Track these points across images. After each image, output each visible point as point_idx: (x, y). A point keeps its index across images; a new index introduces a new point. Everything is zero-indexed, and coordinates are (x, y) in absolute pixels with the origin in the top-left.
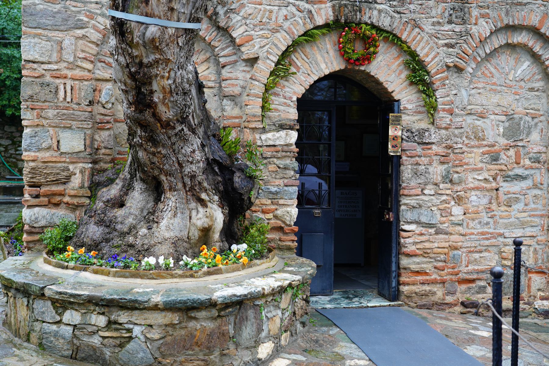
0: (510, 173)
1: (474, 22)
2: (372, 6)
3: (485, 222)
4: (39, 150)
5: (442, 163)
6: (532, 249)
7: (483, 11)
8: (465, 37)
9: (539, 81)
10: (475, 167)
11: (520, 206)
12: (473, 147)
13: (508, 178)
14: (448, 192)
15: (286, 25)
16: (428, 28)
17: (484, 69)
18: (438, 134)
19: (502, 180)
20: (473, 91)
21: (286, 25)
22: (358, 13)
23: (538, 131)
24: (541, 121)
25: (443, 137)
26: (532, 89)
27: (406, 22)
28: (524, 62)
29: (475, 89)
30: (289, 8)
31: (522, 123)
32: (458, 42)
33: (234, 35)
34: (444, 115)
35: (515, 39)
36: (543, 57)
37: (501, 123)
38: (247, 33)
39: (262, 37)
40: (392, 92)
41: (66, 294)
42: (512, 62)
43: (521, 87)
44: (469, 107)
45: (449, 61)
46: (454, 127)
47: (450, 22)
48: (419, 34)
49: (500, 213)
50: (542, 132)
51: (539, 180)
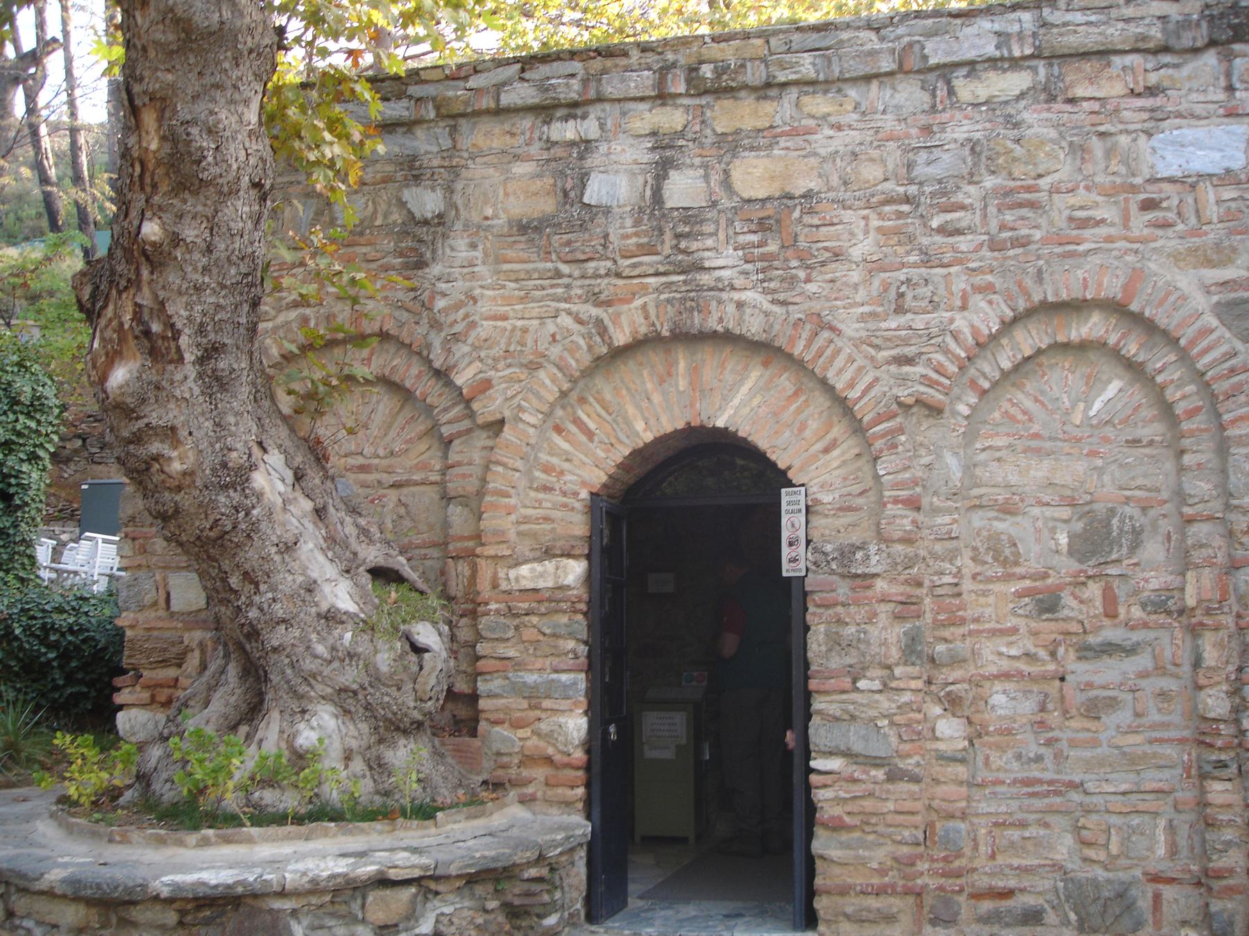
0: (1091, 639)
2: (724, 295)
3: (1032, 755)
4: (142, 609)
5: (898, 617)
6: (1162, 823)
7: (979, 280)
8: (940, 339)
9: (1151, 421)
10: (999, 626)
11: (1124, 717)
12: (989, 580)
13: (1087, 652)
14: (914, 684)
15: (555, 351)
16: (851, 328)
17: (1006, 405)
18: (884, 555)
19: (1072, 655)
20: (983, 457)
21: (555, 351)
22: (696, 313)
23: (1160, 538)
24: (1164, 516)
25: (898, 560)
26: (1135, 442)
27: (800, 319)
28: (1109, 382)
29: (987, 452)
30: (559, 320)
31: (1115, 522)
32: (924, 350)
33: (460, 380)
34: (899, 512)
36: (1150, 368)
37: (1059, 524)
38: (481, 375)
39: (510, 380)
40: (789, 468)
42: (1075, 381)
43: (1106, 440)
44: (976, 492)
45: (903, 393)
46: (932, 537)
47: (900, 310)
48: (831, 341)
49: (1069, 734)
51: (1168, 654)
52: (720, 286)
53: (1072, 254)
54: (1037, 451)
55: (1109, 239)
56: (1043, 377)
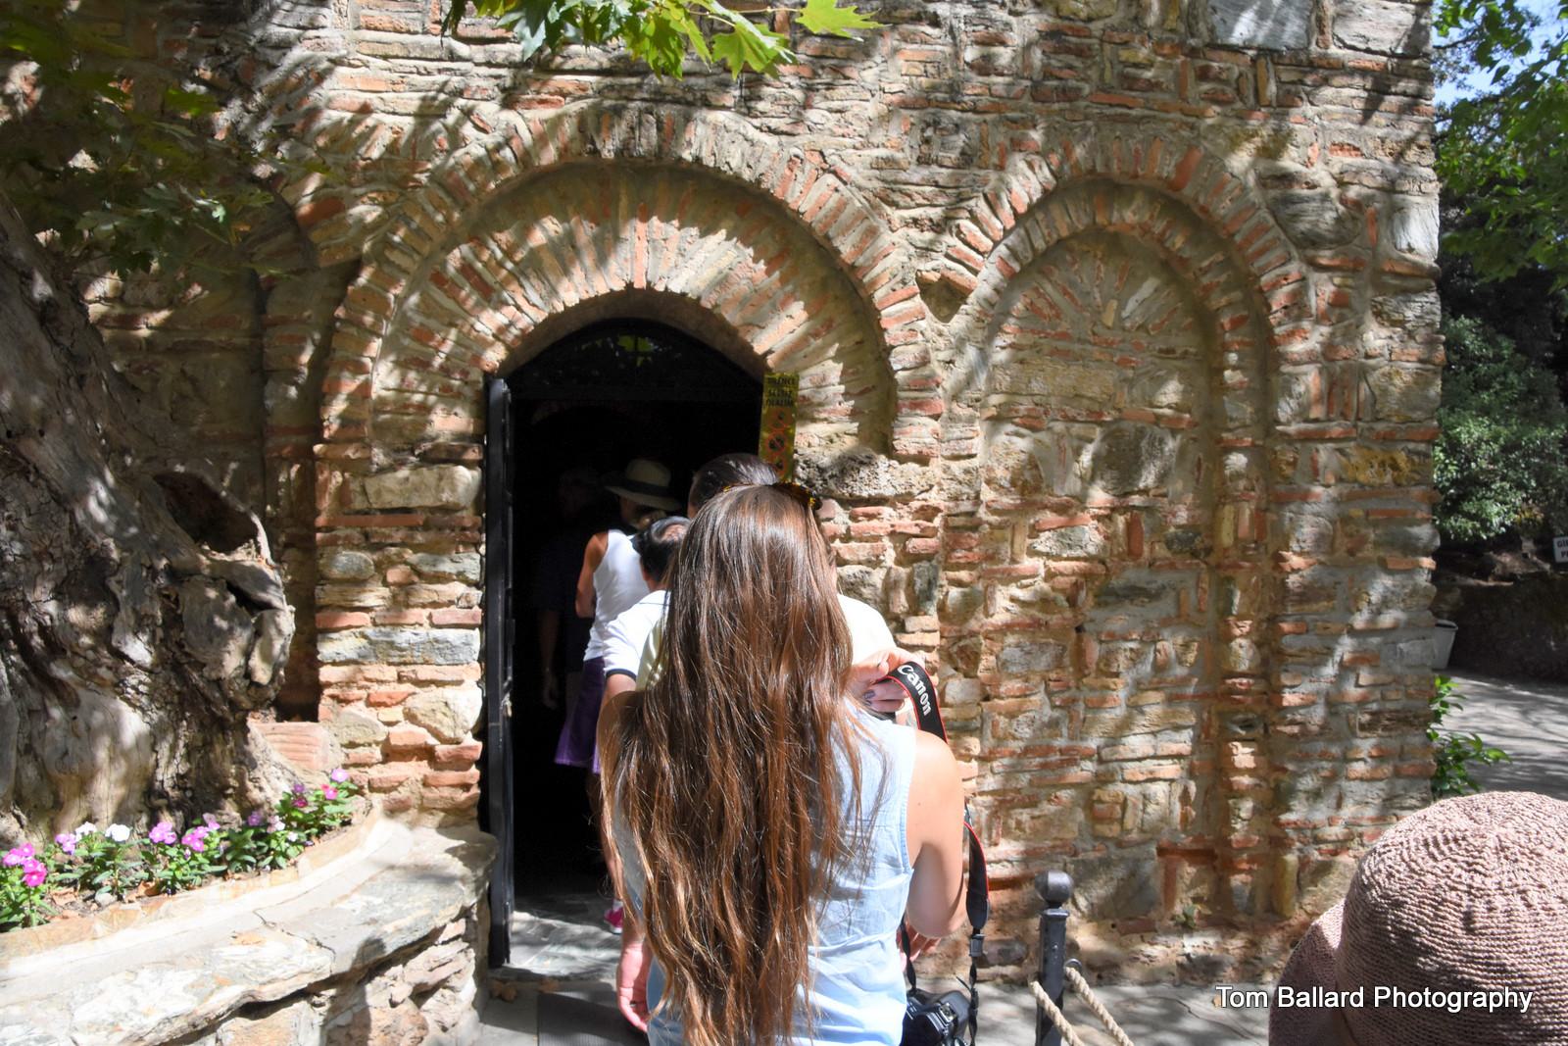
0: (1116, 582)
1: (995, 160)
3: (1046, 719)
18: (898, 474)
28: (1144, 279)
31: (1144, 444)
35: (1116, 215)
38: (325, 191)
43: (1138, 346)
50: (1199, 469)
52: (690, 97)
53: (1124, 119)
54: (1066, 356)
55: (1165, 108)
56: (1073, 264)
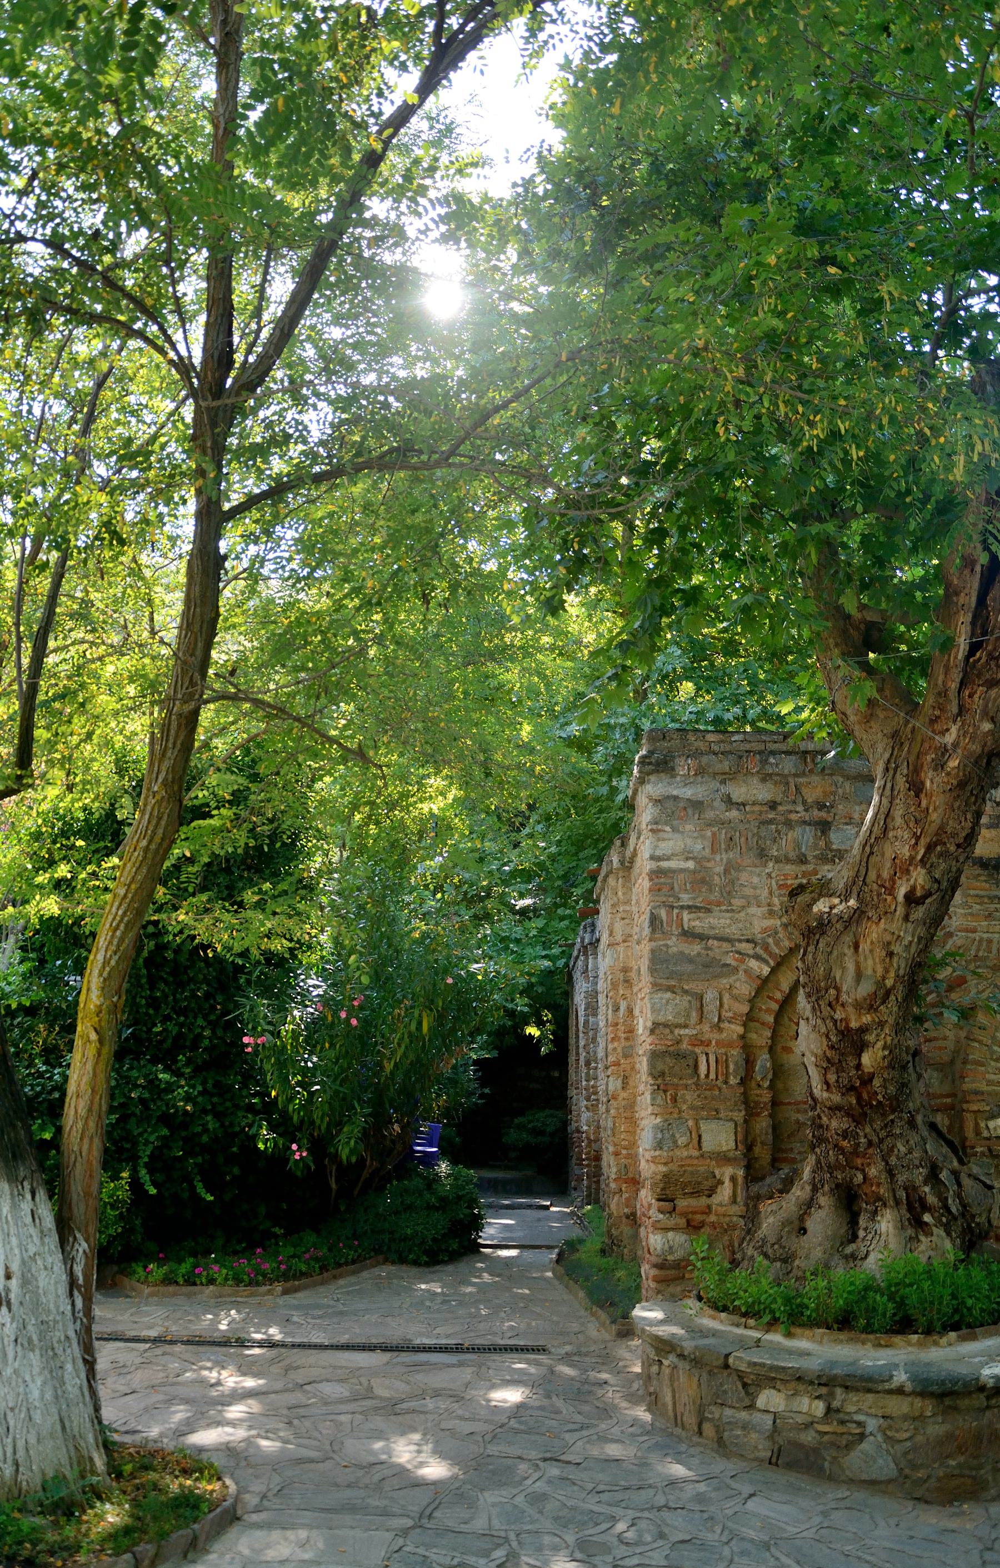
41: (763, 1365)
